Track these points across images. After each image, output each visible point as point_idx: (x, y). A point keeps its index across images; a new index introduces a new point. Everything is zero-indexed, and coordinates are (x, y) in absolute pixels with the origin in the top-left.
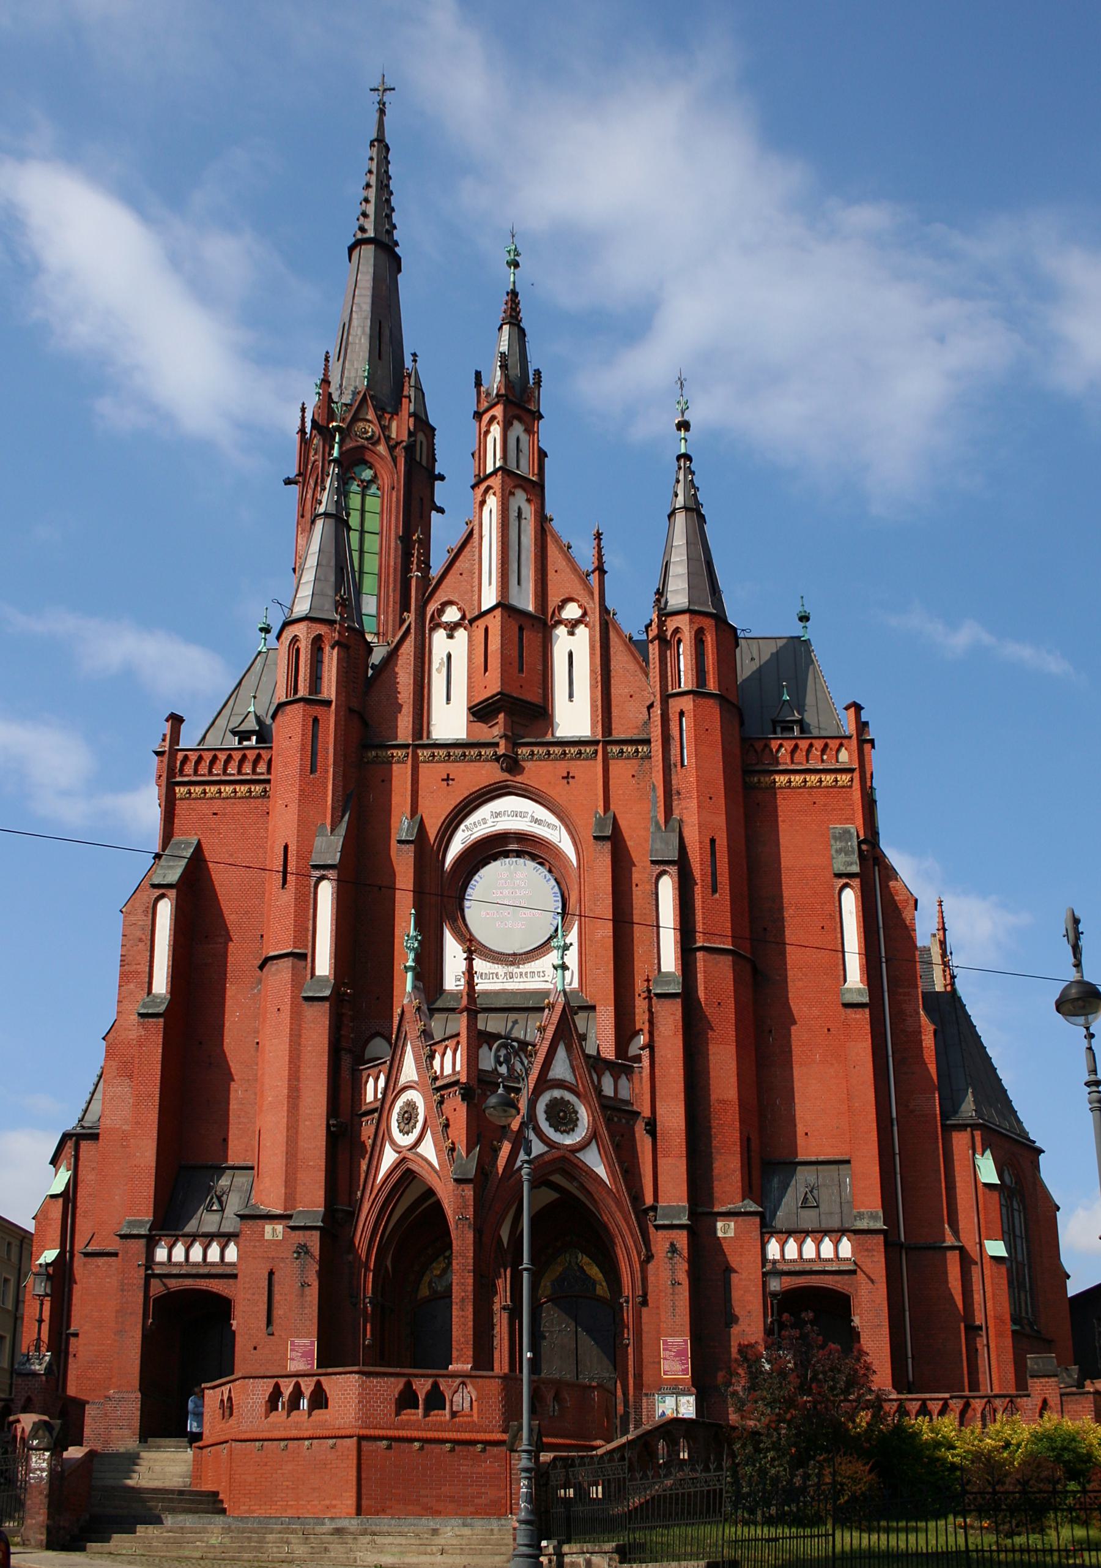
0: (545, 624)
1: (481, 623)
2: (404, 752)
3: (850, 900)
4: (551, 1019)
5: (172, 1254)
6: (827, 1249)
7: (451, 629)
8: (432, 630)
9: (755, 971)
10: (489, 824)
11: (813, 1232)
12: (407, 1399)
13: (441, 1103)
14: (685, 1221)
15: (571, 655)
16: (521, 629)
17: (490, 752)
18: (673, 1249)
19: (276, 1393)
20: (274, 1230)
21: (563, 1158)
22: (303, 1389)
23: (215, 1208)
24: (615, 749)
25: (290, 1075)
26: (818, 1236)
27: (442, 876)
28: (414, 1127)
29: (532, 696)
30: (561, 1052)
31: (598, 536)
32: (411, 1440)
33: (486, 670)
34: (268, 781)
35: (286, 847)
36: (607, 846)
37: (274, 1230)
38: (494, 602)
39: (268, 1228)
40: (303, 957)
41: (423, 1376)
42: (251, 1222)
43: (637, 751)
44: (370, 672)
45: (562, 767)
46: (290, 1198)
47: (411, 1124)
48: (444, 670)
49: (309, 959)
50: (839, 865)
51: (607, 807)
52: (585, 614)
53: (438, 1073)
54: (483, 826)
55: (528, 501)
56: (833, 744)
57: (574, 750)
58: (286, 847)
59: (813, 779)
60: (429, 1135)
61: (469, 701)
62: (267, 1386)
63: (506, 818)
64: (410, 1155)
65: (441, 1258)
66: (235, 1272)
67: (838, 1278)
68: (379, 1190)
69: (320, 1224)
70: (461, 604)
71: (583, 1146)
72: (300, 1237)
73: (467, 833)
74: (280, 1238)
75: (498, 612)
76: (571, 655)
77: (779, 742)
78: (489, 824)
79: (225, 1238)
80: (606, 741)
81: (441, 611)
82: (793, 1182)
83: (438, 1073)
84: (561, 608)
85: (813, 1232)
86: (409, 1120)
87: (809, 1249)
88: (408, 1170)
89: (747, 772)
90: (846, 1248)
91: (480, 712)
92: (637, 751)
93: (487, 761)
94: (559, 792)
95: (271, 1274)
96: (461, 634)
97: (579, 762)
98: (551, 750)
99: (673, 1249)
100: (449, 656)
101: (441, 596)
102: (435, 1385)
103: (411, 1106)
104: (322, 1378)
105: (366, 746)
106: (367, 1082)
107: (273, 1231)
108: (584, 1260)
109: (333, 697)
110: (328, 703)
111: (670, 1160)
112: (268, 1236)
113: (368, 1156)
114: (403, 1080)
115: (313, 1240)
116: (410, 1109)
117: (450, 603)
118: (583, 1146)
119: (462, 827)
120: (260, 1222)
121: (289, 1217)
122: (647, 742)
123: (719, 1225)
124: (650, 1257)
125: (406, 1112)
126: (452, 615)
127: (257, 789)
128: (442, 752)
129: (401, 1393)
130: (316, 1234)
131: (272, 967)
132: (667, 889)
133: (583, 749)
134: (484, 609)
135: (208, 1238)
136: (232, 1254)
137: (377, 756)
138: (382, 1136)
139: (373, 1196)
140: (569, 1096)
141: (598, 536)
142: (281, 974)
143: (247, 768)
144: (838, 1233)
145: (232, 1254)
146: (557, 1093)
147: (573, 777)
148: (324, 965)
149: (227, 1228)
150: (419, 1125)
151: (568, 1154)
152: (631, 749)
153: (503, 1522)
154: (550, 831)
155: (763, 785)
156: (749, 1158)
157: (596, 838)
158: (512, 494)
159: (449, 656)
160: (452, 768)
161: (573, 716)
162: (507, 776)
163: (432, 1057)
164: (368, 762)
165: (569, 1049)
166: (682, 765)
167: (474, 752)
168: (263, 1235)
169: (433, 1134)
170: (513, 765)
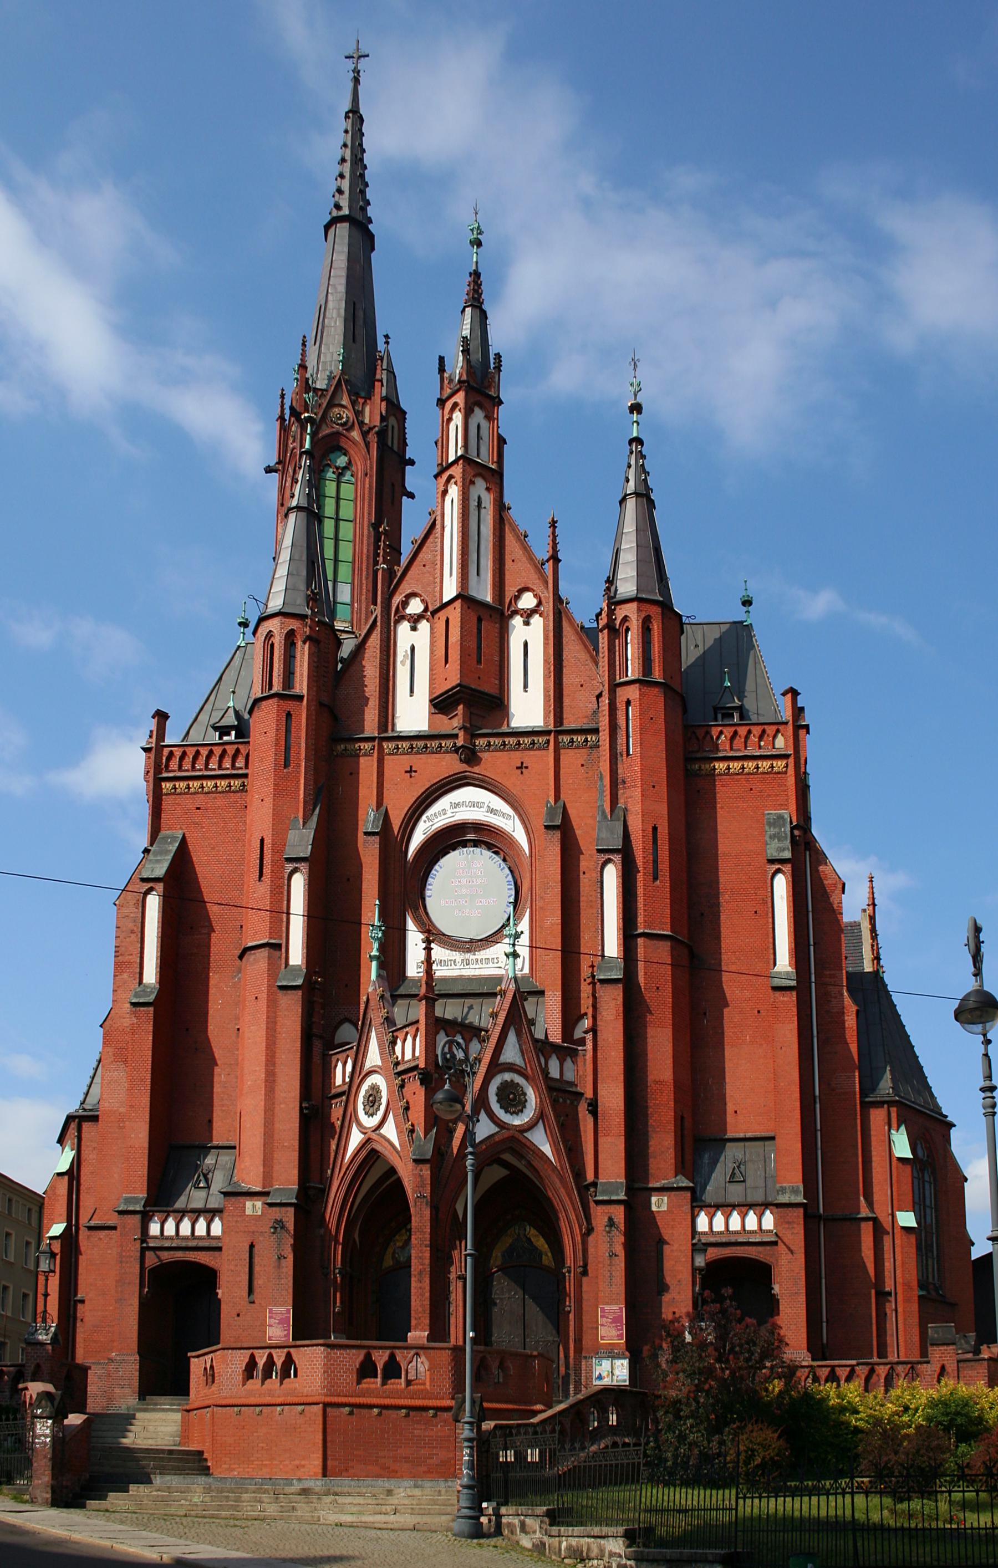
0: (503, 614)
1: (442, 615)
2: (370, 744)
3: (781, 885)
4: (502, 1005)
5: (164, 1228)
6: (751, 1221)
7: (415, 621)
8: (397, 622)
9: (692, 955)
10: (449, 814)
11: (739, 1205)
12: (367, 1369)
13: (402, 1086)
14: (622, 1196)
15: (526, 645)
16: (480, 620)
18: (611, 1223)
19: (251, 1366)
20: (254, 1206)
21: (512, 1138)
22: (275, 1359)
23: (201, 1185)
24: (566, 739)
25: (267, 1060)
26: (744, 1209)
27: (405, 867)
28: (378, 1109)
29: (489, 688)
30: (512, 1037)
31: (553, 524)
32: (371, 1407)
33: (446, 662)
34: (245, 776)
35: (262, 841)
36: (558, 834)
37: (254, 1206)
38: (454, 594)
39: (249, 1204)
40: (278, 947)
41: (381, 1348)
42: (233, 1199)
43: (586, 741)
44: (340, 666)
46: (268, 1176)
47: (376, 1107)
48: (408, 662)
49: (283, 950)
50: (772, 852)
51: (557, 797)
52: (539, 604)
53: (400, 1058)
54: (443, 817)
55: (488, 489)
56: (770, 730)
57: (527, 740)
58: (262, 841)
59: (750, 765)
60: (391, 1118)
61: (431, 693)
62: (244, 1357)
63: (464, 808)
64: (374, 1136)
65: (404, 1231)
66: (220, 1245)
67: (760, 1248)
68: (347, 1169)
69: (294, 1201)
70: (424, 596)
72: (276, 1213)
73: (428, 824)
74: (260, 1213)
75: (458, 604)
76: (526, 645)
77: (720, 729)
78: (449, 814)
79: (211, 1213)
80: (558, 731)
81: (405, 604)
82: (722, 1158)
83: (400, 1058)
84: (517, 598)
85: (739, 1205)
86: (374, 1102)
87: (735, 1222)
88: (373, 1150)
89: (689, 759)
90: (769, 1221)
91: (441, 704)
92: (586, 741)
94: (512, 782)
95: (252, 1246)
96: (424, 626)
97: (532, 753)
98: (507, 740)
99: (611, 1223)
100: (413, 649)
101: (405, 588)
102: (392, 1357)
103: (375, 1089)
104: (292, 1350)
105: (336, 739)
106: (336, 1066)
107: (254, 1207)
108: (532, 1232)
109: (305, 692)
110: (300, 698)
111: (609, 1139)
112: (249, 1211)
113: (337, 1136)
114: (368, 1065)
115: (289, 1216)
116: (375, 1092)
117: (414, 595)
118: (531, 1126)
119: (424, 818)
120: (241, 1199)
121: (267, 1194)
122: (596, 731)
123: (654, 1199)
124: (590, 1230)
125: (371, 1095)
126: (415, 607)
127: (236, 783)
128: (406, 745)
129: (362, 1364)
130: (291, 1210)
131: (250, 957)
132: (611, 876)
133: (536, 739)
135: (196, 1214)
136: (217, 1228)
137: (346, 750)
138: (349, 1118)
139: (341, 1175)
140: (518, 1079)
141: (553, 524)
142: (259, 961)
143: (227, 763)
144: (761, 1207)
145: (217, 1228)
146: (507, 1076)
147: (526, 767)
148: (297, 955)
149: (213, 1204)
150: (383, 1108)
151: (517, 1135)
152: (579, 739)
153: (450, 1484)
154: (504, 820)
155: (703, 772)
156: (682, 1136)
157: (547, 827)
158: (472, 483)
159: (413, 649)
160: (417, 761)
161: (527, 708)
162: (464, 767)
163: (394, 1043)
164: (337, 756)
165: (519, 1034)
166: (628, 754)
167: (435, 744)
169: (394, 1116)
170: (470, 756)
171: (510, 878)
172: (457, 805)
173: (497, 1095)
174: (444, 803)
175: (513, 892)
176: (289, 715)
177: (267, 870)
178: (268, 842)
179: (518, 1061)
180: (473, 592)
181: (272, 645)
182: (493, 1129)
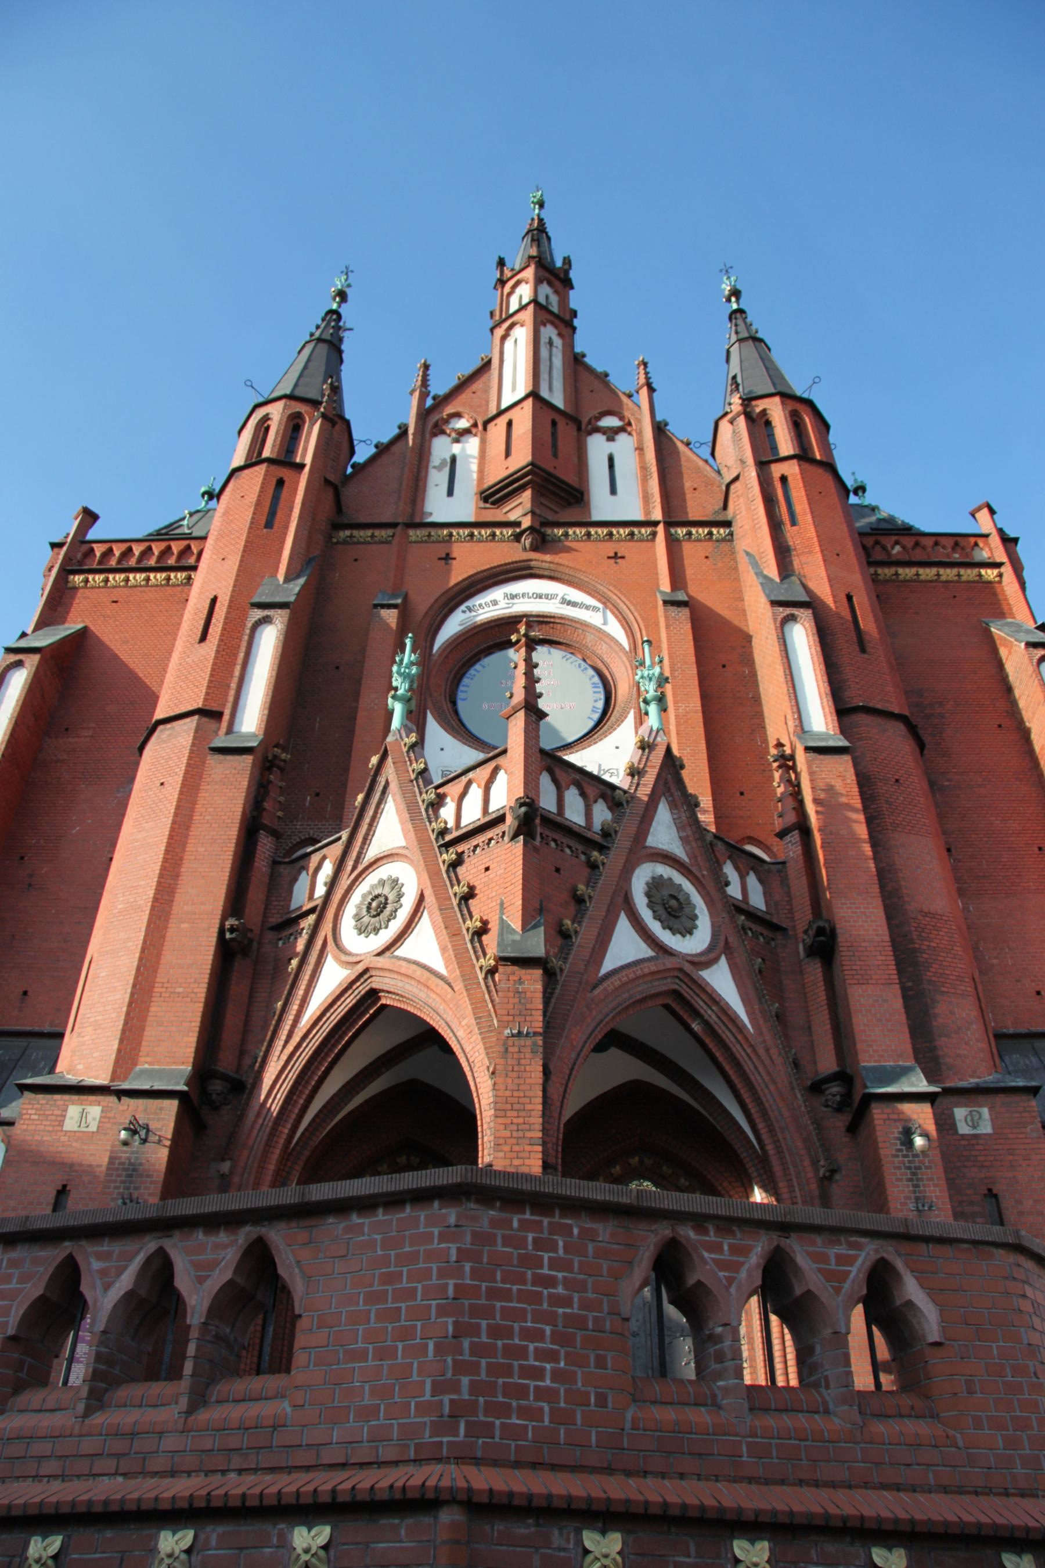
2: (390, 532)
17: (508, 532)
24: (681, 532)
25: (163, 868)
33: (508, 454)
44: (349, 470)
45: (610, 548)
54: (492, 608)
57: (624, 532)
71: (705, 960)
74: (93, 1128)
77: (894, 538)
84: (598, 418)
92: (710, 533)
98: (592, 531)
105: (337, 527)
118: (705, 960)
119: (463, 607)
127: (181, 576)
133: (636, 531)
137: (351, 536)
139: (284, 1057)
147: (623, 557)
151: (687, 967)
152: (703, 531)
164: (337, 543)
167: (485, 532)
168: (61, 1123)
171: (596, 679)
172: (513, 597)
173: (648, 895)
174: (497, 593)
175: (602, 696)
176: (280, 483)
179: (678, 850)
180: (544, 393)
181: (267, 429)
182: (642, 950)
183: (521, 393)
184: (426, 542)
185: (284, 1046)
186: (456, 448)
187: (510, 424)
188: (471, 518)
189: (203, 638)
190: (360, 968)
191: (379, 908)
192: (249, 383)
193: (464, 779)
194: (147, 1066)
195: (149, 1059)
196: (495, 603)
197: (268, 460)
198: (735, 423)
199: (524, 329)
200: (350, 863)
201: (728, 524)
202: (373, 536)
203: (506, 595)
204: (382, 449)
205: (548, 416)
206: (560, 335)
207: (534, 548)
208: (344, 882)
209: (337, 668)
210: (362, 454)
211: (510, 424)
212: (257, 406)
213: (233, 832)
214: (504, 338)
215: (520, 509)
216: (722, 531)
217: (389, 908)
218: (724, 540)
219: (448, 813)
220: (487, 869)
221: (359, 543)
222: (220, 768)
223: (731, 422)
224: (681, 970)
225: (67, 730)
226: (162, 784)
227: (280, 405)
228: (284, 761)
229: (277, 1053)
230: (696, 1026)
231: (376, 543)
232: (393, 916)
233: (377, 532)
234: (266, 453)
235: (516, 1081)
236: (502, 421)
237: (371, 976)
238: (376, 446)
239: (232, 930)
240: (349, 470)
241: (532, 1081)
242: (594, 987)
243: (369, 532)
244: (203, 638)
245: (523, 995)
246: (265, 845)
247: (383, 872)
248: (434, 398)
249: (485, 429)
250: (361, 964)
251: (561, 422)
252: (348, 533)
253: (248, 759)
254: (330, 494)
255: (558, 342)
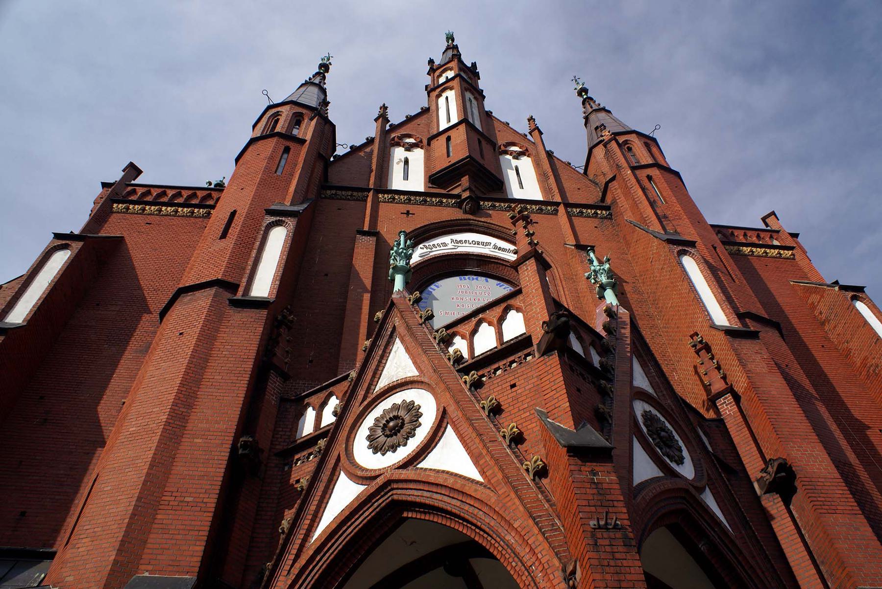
7: (409, 148)
33: (448, 156)
44: (332, 159)
47: (394, 440)
58: (233, 214)
68: (318, 551)
78: (450, 246)
93: (447, 206)
119: (421, 246)
134: (441, 129)
137: (336, 194)
139: (296, 570)
152: (590, 212)
170: (476, 210)
172: (457, 242)
174: (447, 239)
177: (234, 231)
178: (238, 221)
183: (454, 120)
184: (391, 202)
185: (295, 561)
186: (408, 154)
187: (449, 139)
188: (423, 190)
189: (224, 236)
190: (380, 481)
191: (396, 428)
192: (265, 92)
193: (474, 320)
194: (147, 574)
195: (150, 567)
196: (445, 244)
197: (279, 135)
198: (608, 146)
199: (453, 92)
200: (361, 393)
201: (607, 208)
202: (351, 196)
203: (452, 241)
204: (354, 150)
205: (475, 137)
206: (475, 98)
207: (472, 212)
208: (356, 409)
209: (326, 275)
210: (340, 151)
211: (449, 139)
212: (269, 108)
213: (249, 366)
214: (439, 96)
215: (462, 187)
216: (604, 212)
217: (407, 427)
218: (606, 218)
219: (460, 345)
220: (513, 386)
221: (341, 199)
222: (238, 317)
223: (605, 146)
224: (687, 491)
225: (98, 305)
226: (181, 334)
227: (288, 107)
228: (292, 322)
229: (287, 568)
230: (702, 547)
231: (354, 200)
232: (411, 434)
233: (355, 194)
234: (278, 129)
235: (616, 577)
236: (442, 139)
237: (393, 489)
238: (351, 147)
239: (245, 445)
240: (332, 159)
241: (635, 577)
242: (635, 497)
243: (350, 193)
244: (224, 236)
245: (600, 486)
246: (274, 385)
247: (397, 398)
248: (390, 126)
249: (429, 144)
250: (382, 477)
251: (484, 143)
252: (334, 192)
253: (265, 313)
254: (319, 167)
255: (474, 102)
